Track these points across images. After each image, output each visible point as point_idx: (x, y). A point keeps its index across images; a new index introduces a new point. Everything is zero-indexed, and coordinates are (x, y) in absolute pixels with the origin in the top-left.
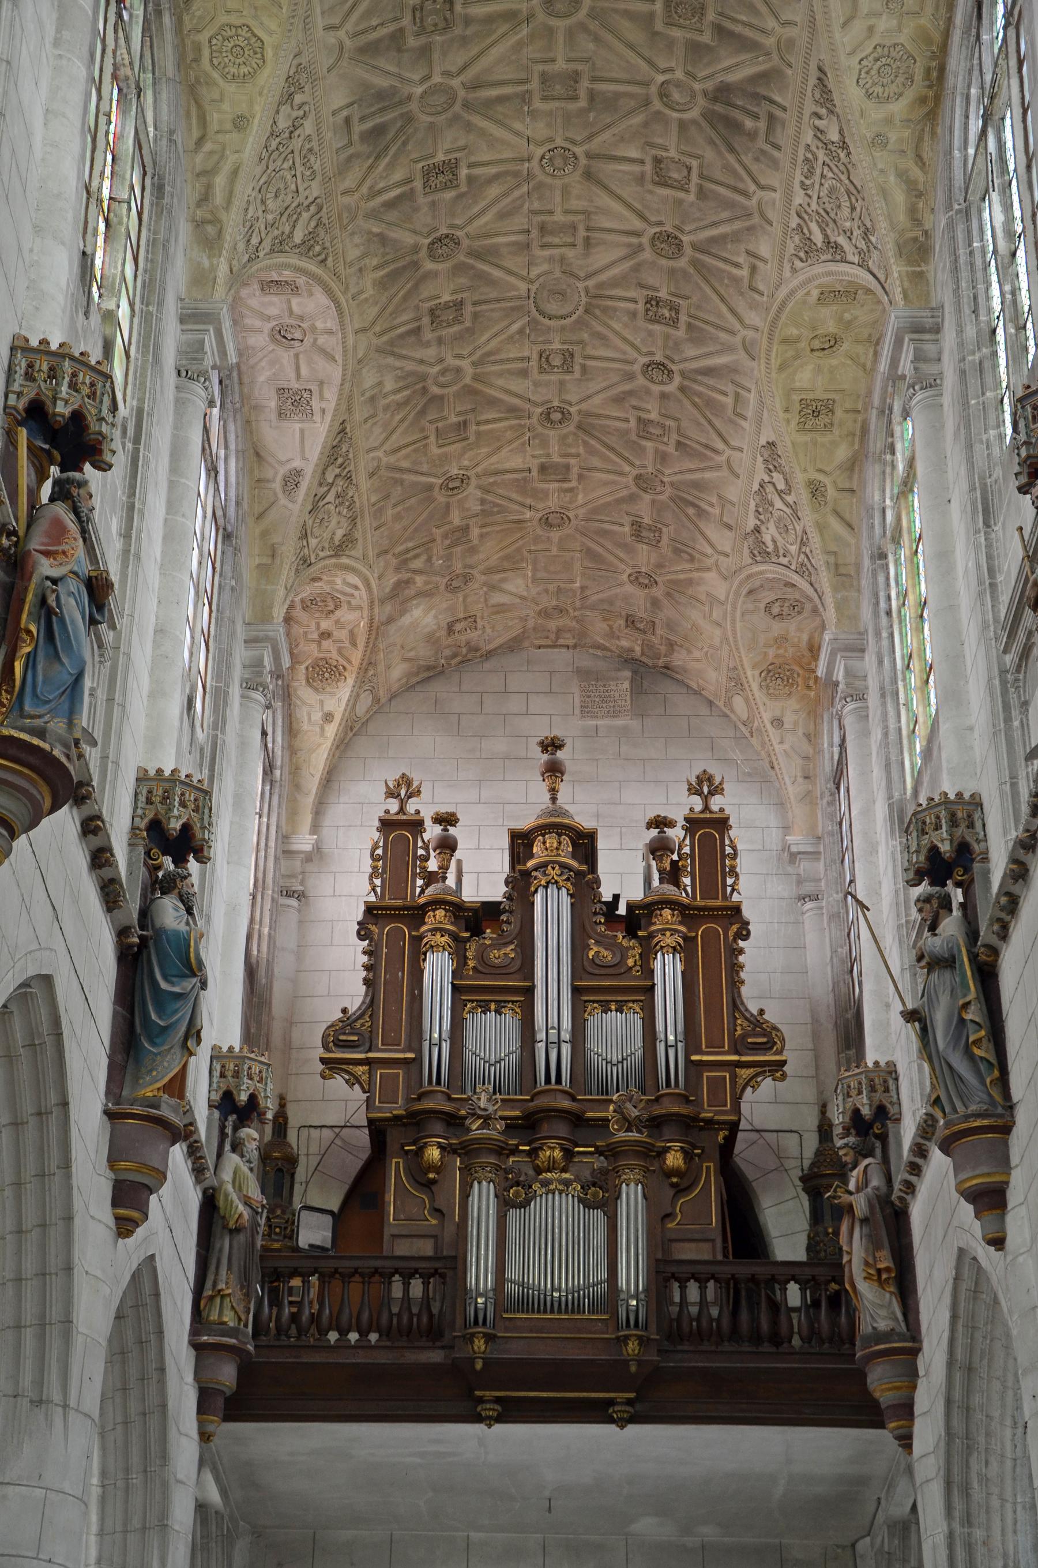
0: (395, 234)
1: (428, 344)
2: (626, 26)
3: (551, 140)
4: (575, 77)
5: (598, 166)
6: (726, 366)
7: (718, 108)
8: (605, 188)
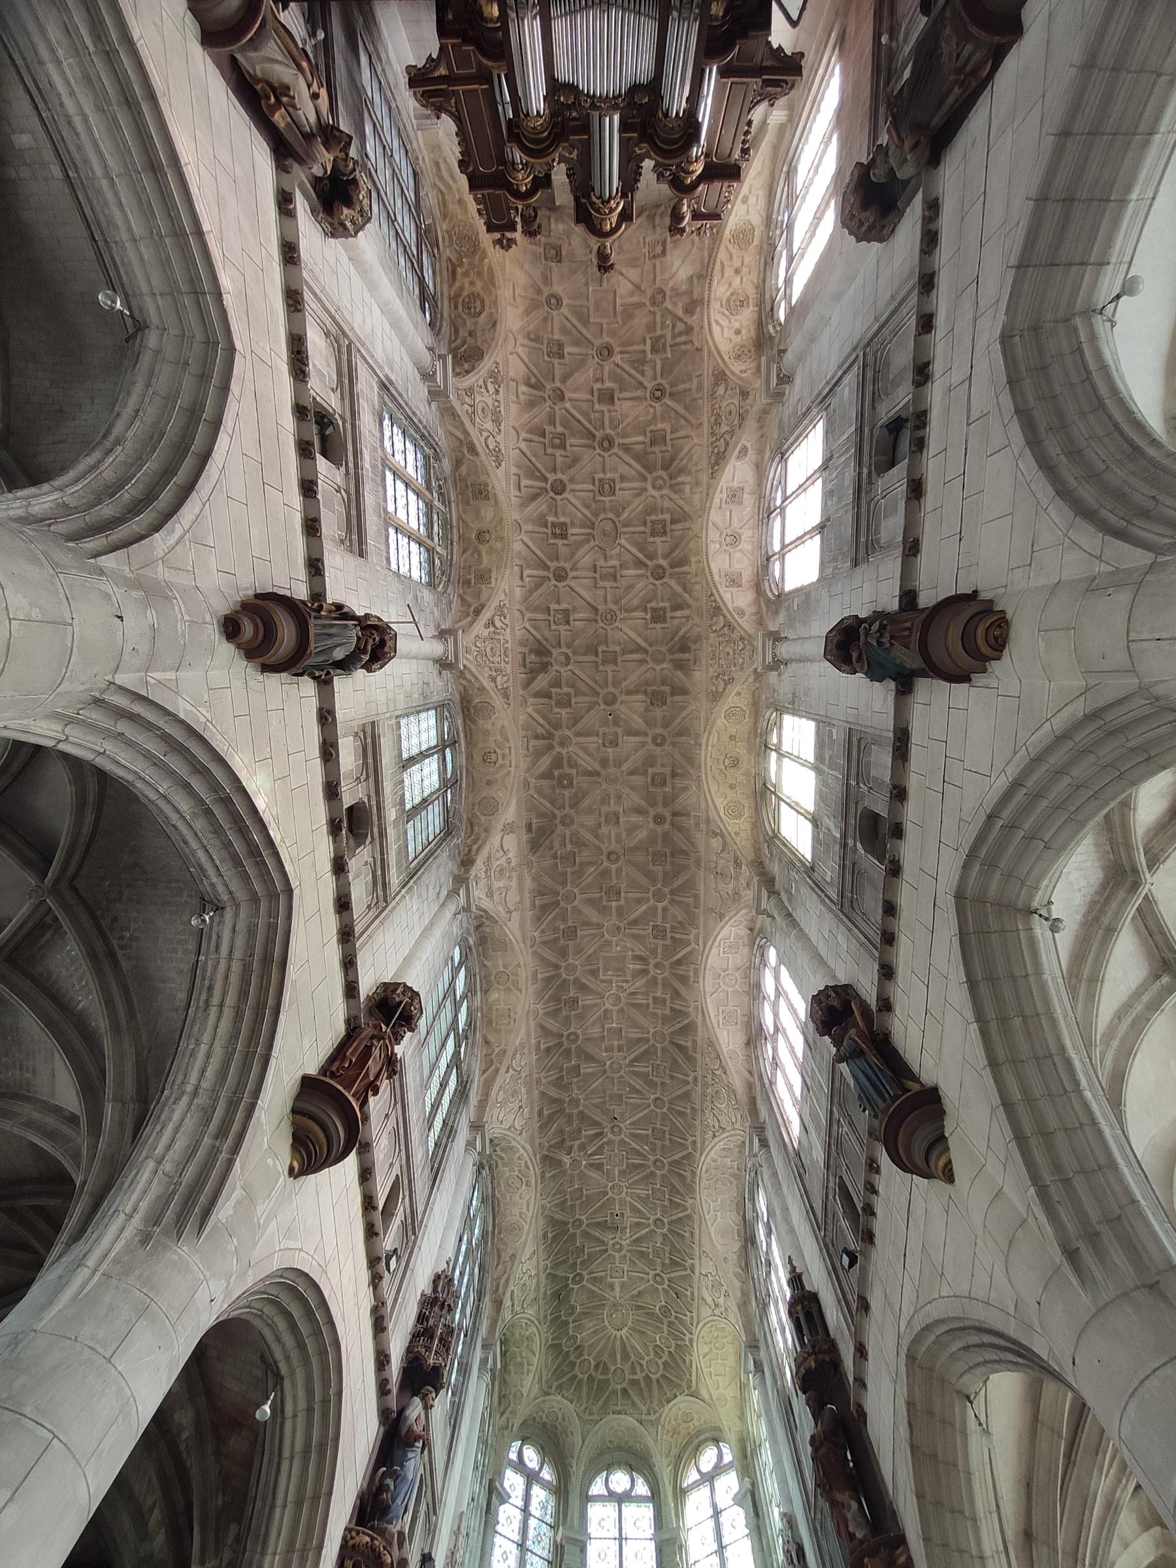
0: (678, 589)
1: (668, 510)
2: (585, 689)
4: (604, 662)
5: (592, 616)
6: (527, 506)
7: (545, 659)
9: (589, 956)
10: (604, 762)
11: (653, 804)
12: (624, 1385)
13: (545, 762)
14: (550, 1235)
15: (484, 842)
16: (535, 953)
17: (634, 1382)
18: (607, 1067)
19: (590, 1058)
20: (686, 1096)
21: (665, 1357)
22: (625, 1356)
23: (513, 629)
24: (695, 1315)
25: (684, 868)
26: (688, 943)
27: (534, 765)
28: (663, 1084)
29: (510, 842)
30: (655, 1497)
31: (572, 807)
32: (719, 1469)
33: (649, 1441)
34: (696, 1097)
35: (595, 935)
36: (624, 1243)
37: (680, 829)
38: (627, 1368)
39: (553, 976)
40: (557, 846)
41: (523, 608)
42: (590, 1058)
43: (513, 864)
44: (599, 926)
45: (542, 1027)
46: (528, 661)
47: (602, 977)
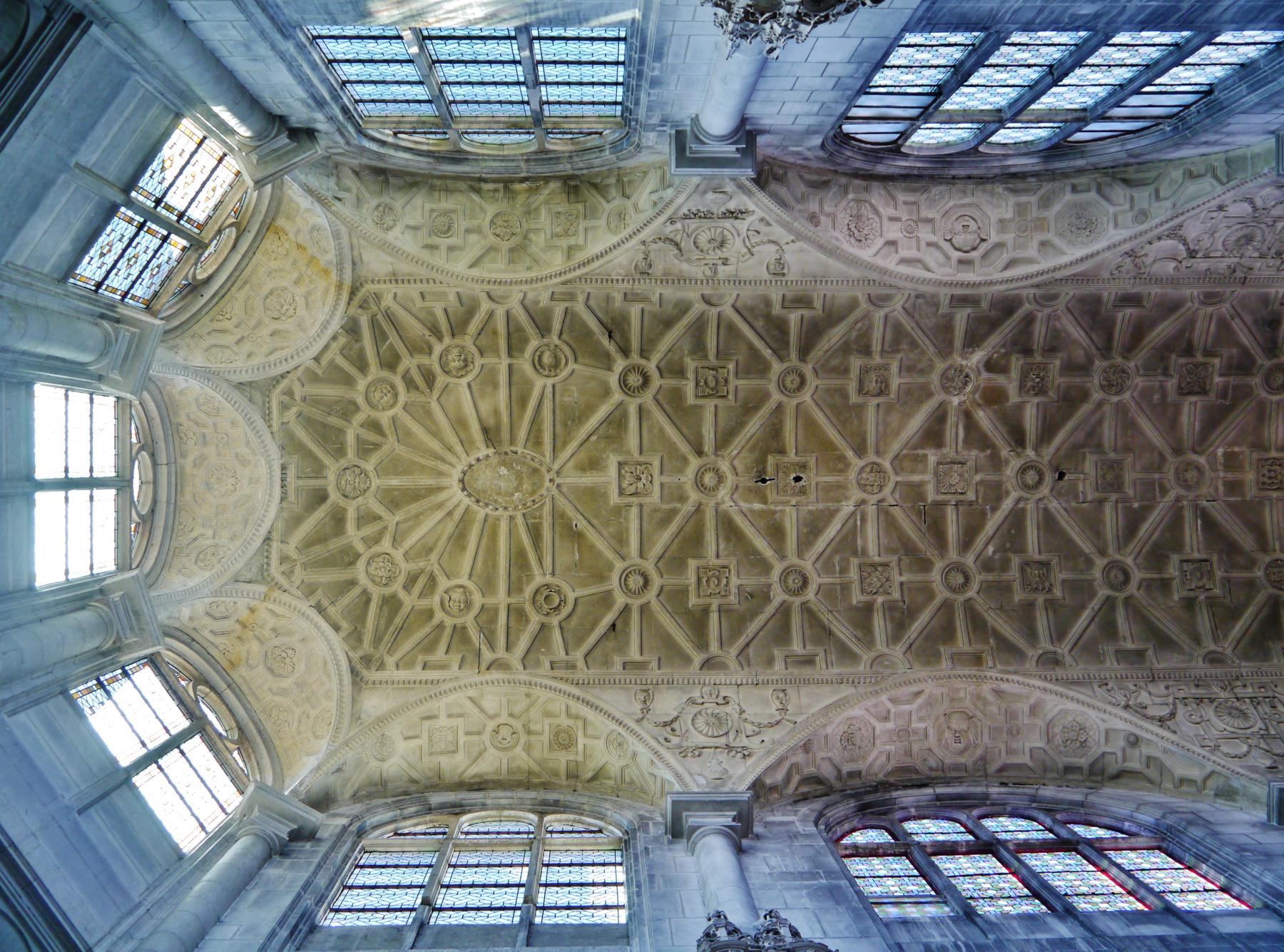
12: (334, 496)
17: (338, 519)
19: (1213, 420)
22: (394, 500)
36: (723, 493)
42: (1213, 420)
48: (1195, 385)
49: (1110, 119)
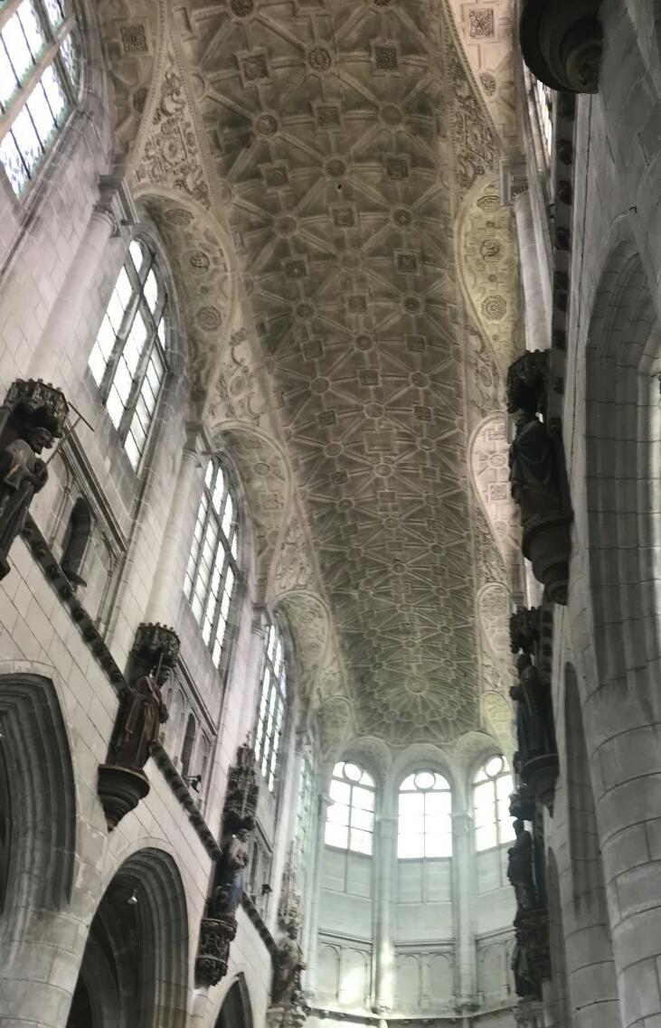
2: (302, 158)
3: (328, 76)
4: (322, 121)
8: (287, 40)
9: (352, 436)
10: (340, 243)
11: (404, 288)
12: (426, 725)
13: (268, 253)
14: (347, 645)
15: (213, 365)
16: (293, 444)
17: (434, 723)
18: (383, 523)
20: (462, 547)
21: (459, 708)
23: (192, 103)
24: (480, 687)
25: (444, 356)
26: (453, 427)
27: (254, 259)
28: (440, 536)
29: (244, 352)
30: (453, 790)
31: (308, 295)
32: (501, 774)
33: (447, 758)
34: (471, 546)
35: (355, 417)
37: (437, 317)
38: (427, 714)
39: (315, 460)
40: (298, 338)
41: (199, 68)
43: (251, 370)
44: (359, 409)
45: (312, 502)
46: (221, 140)
47: (368, 452)
48: (354, 528)
49: (270, 688)
